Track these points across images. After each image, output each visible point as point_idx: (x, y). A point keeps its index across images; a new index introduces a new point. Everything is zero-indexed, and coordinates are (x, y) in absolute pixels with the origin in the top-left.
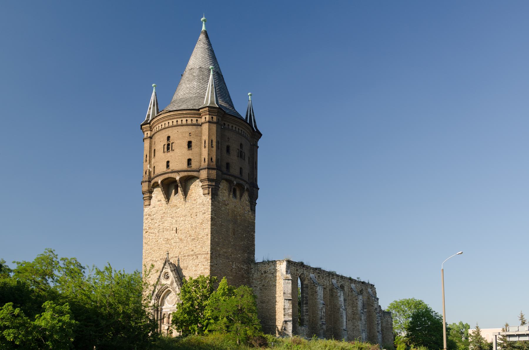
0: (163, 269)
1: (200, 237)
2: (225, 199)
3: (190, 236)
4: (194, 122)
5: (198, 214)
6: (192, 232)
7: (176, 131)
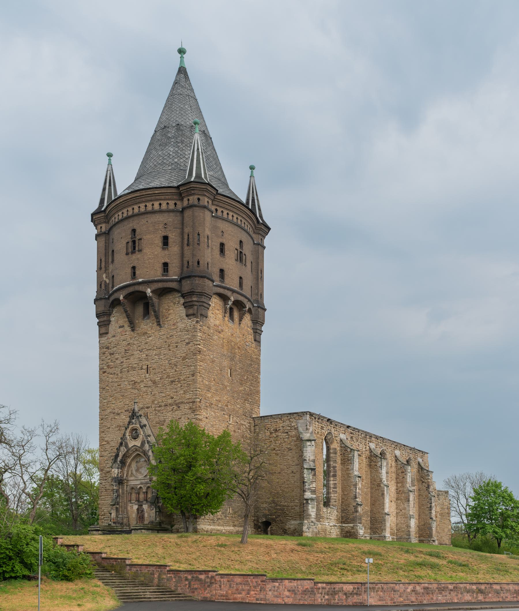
0: (128, 425)
1: (182, 378)
2: (217, 322)
3: (168, 376)
5: (179, 345)
6: (171, 372)
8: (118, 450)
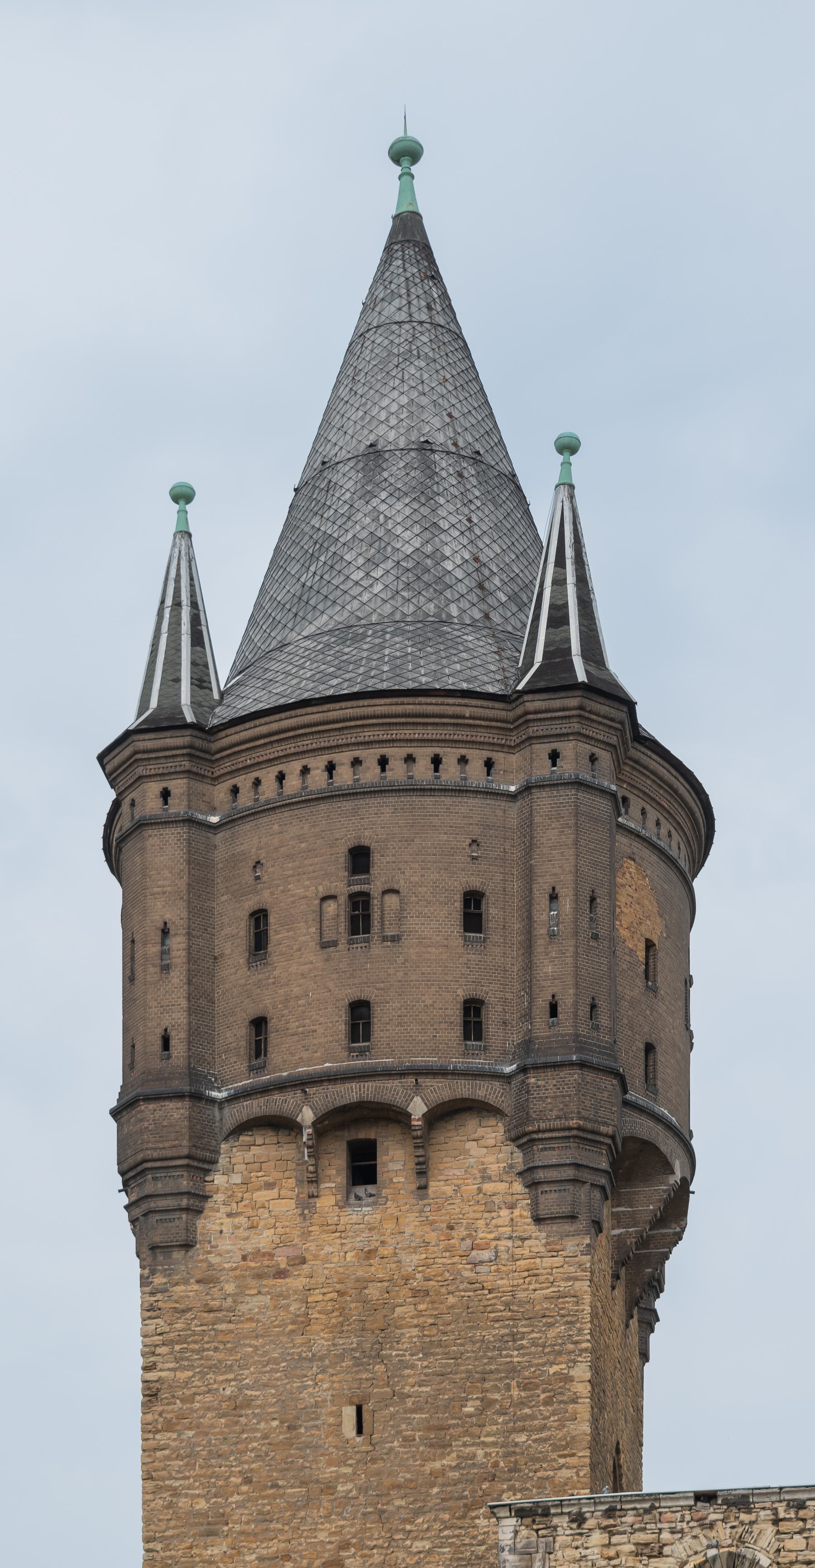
2: (264, 1239)
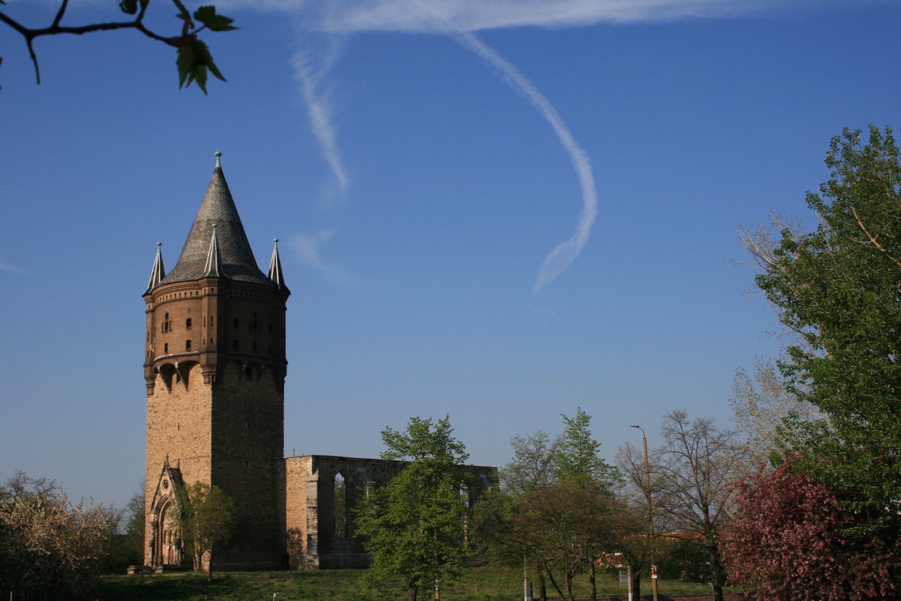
3: (192, 434)
4: (194, 295)
6: (194, 430)
7: (174, 307)
8: (155, 498)
